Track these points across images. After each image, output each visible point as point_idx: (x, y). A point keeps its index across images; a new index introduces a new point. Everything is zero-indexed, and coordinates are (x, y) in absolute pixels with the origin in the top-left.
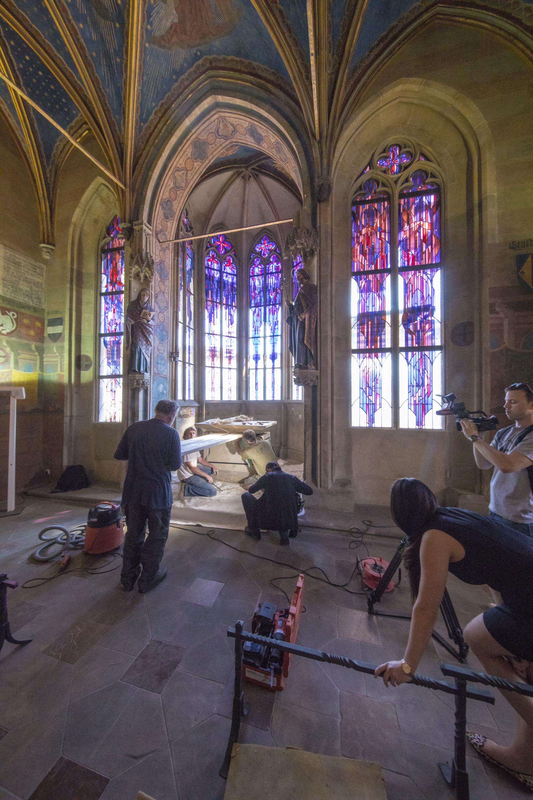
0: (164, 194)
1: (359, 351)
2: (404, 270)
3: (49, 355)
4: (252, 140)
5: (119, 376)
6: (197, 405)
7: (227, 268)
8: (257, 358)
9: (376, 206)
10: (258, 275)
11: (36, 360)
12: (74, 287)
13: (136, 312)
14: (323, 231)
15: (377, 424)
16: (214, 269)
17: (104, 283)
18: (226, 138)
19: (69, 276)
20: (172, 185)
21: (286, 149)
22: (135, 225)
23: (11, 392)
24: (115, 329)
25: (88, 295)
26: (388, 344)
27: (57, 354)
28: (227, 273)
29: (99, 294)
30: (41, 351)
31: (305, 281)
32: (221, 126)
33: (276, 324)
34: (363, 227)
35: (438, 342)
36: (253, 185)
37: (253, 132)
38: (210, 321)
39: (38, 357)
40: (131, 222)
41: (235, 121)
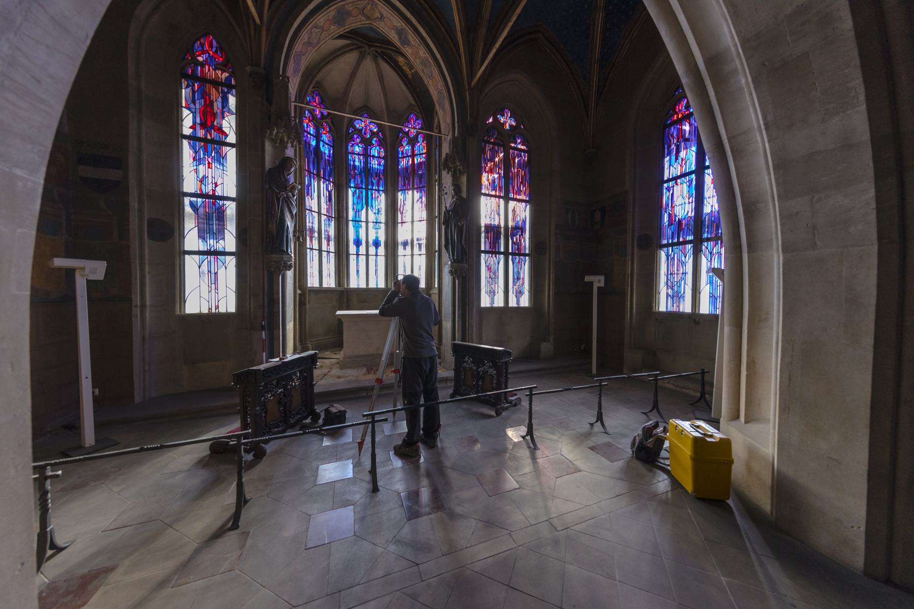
0: (298, 47)
1: (485, 252)
4: (396, 37)
8: (358, 243)
18: (368, 18)
20: (306, 40)
24: (214, 191)
26: (502, 250)
32: (369, 7)
41: (385, 13)
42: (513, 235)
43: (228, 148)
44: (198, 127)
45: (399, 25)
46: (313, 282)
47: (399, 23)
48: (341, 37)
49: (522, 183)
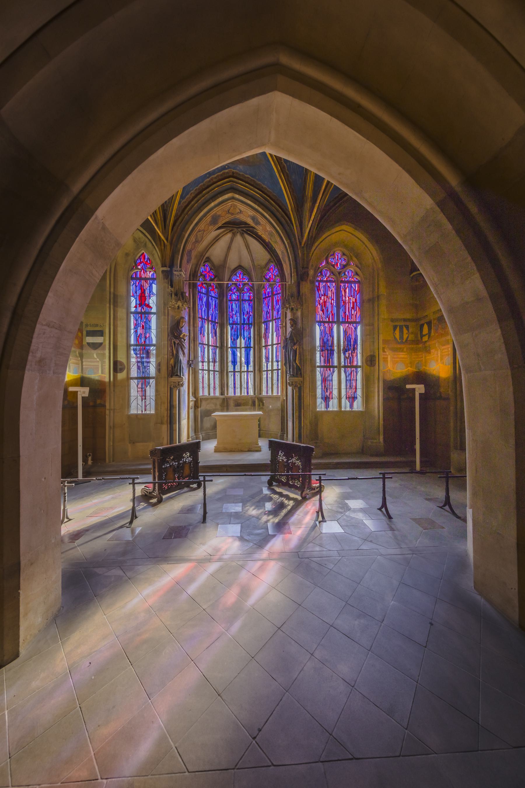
0: (189, 247)
1: (320, 367)
2: (344, 322)
3: (89, 360)
4: (252, 221)
5: (149, 378)
6: (195, 399)
7: (212, 292)
9: (329, 284)
10: (235, 300)
11: (79, 364)
12: (112, 306)
13: (174, 332)
14: (303, 298)
15: (330, 409)
16: (203, 293)
17: (133, 304)
18: (232, 214)
19: (108, 298)
20: (194, 241)
21: (278, 239)
22: (175, 271)
23: (77, 392)
24: (145, 342)
25: (121, 313)
26: (336, 364)
27: (98, 360)
28: (212, 296)
29: (128, 313)
30: (81, 356)
31: (294, 325)
33: (249, 338)
34: (322, 295)
35: (360, 364)
36: (239, 238)
37: (253, 218)
38: (201, 333)
39: (80, 361)
40: (169, 267)
41: (242, 209)
42: (345, 351)
43: (152, 315)
44: (138, 306)
45: (252, 214)
46: (203, 392)
47: (251, 213)
48: (219, 228)
49: (353, 308)
